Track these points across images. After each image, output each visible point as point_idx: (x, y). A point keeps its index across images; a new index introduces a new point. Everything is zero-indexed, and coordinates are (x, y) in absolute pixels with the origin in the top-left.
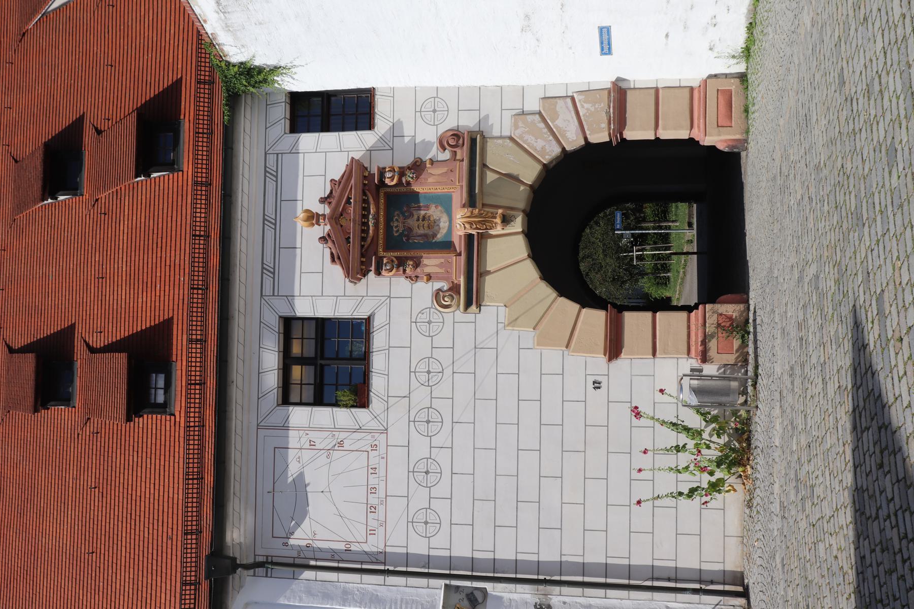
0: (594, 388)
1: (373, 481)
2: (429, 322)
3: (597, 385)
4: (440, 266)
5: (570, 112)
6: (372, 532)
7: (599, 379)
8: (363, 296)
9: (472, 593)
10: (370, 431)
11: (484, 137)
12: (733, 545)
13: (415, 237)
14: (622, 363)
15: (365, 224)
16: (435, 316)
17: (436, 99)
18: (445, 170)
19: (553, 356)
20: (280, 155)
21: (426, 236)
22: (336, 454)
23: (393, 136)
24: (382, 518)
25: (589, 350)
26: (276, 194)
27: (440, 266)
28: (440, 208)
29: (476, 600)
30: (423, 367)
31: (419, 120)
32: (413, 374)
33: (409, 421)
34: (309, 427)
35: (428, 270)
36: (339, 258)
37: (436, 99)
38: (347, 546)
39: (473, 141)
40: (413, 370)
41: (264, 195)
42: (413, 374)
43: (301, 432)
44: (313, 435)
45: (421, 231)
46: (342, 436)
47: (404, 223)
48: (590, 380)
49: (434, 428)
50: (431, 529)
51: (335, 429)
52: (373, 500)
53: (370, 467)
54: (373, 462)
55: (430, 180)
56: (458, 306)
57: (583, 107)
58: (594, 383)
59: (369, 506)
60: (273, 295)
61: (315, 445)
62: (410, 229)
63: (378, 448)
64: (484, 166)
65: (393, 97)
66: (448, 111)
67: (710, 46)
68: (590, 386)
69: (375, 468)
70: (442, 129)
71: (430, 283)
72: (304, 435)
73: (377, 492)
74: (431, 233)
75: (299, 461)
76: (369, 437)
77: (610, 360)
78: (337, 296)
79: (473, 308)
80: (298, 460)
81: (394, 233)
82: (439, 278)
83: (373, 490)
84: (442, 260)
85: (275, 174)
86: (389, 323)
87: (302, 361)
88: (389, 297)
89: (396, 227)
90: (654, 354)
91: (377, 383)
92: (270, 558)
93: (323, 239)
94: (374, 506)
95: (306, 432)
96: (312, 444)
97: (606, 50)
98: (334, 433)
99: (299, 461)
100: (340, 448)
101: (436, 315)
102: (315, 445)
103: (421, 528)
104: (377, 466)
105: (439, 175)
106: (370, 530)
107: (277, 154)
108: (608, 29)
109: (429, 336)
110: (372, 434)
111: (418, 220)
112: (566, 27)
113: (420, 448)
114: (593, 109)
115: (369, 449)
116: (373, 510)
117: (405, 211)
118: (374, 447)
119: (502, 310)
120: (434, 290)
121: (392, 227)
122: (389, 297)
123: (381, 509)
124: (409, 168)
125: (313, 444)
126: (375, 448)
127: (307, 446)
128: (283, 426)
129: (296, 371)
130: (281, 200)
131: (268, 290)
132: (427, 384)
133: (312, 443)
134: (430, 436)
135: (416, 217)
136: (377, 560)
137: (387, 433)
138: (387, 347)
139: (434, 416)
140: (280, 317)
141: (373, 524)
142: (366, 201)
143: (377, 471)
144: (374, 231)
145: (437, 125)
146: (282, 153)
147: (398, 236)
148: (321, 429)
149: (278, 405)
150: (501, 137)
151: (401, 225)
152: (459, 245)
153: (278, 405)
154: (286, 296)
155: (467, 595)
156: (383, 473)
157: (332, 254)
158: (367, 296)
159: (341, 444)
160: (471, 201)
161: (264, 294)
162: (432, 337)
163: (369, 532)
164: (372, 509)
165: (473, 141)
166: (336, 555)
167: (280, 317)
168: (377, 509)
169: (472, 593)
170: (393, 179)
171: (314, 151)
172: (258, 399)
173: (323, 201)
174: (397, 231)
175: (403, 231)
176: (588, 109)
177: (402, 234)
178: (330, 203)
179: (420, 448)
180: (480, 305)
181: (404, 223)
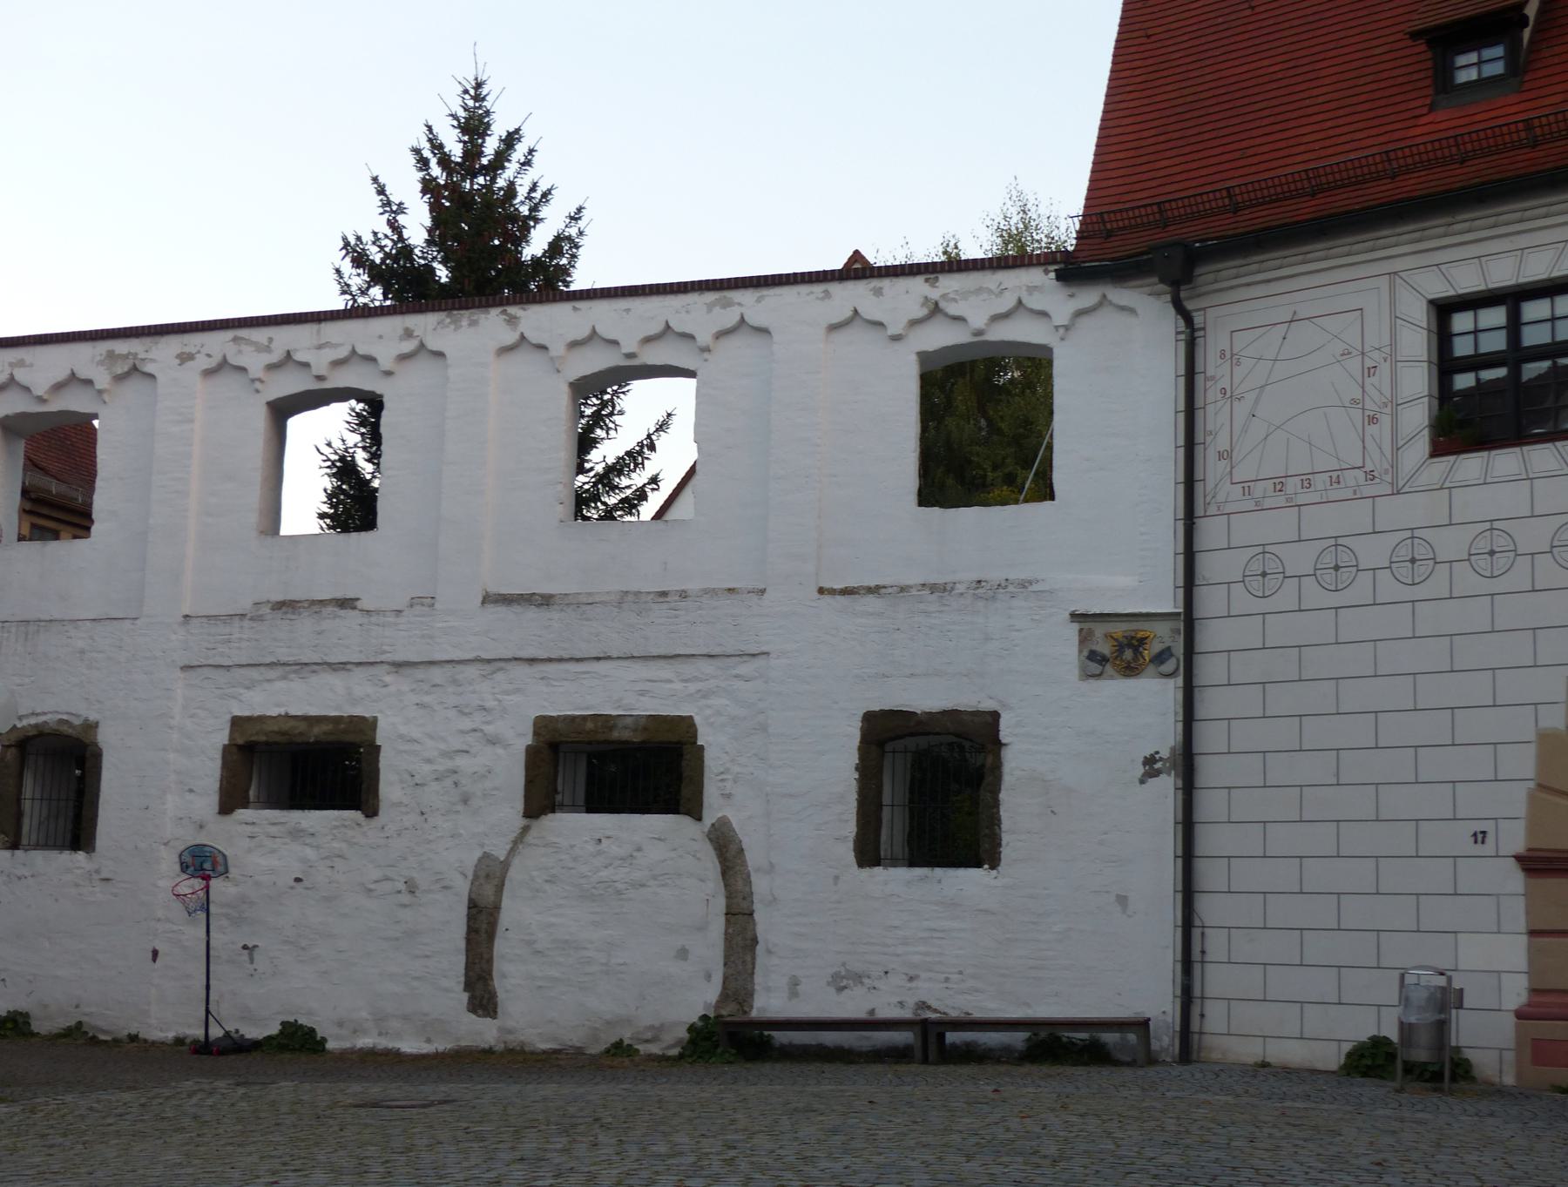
0: (1475, 835)
1: (1320, 481)
3: (1480, 837)
6: (1247, 489)
7: (1490, 839)
9: (1172, 655)
10: (1394, 466)
12: (1250, 1052)
14: (1516, 880)
19: (1523, 763)
22: (1357, 414)
24: (1268, 503)
25: (1533, 825)
29: (1162, 663)
30: (1501, 542)
34: (1396, 361)
38: (1225, 453)
40: (1496, 525)
43: (1387, 350)
44: (1385, 368)
46: (1386, 420)
48: (1488, 826)
49: (1404, 571)
51: (1395, 405)
52: (1292, 485)
53: (1339, 473)
54: (1350, 478)
58: (1484, 833)
59: (1283, 480)
63: (1370, 482)
68: (1480, 826)
69: (1339, 482)
72: (1384, 355)
73: (1305, 490)
75: (1342, 355)
76: (1387, 466)
83: (1307, 484)
87: (1514, 326)
91: (1471, 465)
92: (1201, 333)
94: (1283, 488)
95: (1389, 358)
99: (1342, 355)
102: (1369, 376)
104: (1342, 485)
106: (1249, 487)
110: (1391, 470)
113: (1372, 552)
115: (1368, 469)
116: (1278, 487)
118: (1371, 476)
123: (1281, 501)
125: (1371, 374)
126: (1368, 476)
127: (1369, 363)
129: (1495, 316)
133: (1372, 370)
136: (1209, 504)
137: (1393, 494)
138: (1531, 476)
139: (1422, 569)
141: (1258, 490)
143: (1335, 485)
155: (1169, 648)
156: (1333, 495)
159: (1373, 420)
163: (1246, 485)
164: (1280, 487)
166: (1212, 437)
168: (1280, 493)
169: (1172, 655)
172: (1437, 265)
179: (1372, 552)
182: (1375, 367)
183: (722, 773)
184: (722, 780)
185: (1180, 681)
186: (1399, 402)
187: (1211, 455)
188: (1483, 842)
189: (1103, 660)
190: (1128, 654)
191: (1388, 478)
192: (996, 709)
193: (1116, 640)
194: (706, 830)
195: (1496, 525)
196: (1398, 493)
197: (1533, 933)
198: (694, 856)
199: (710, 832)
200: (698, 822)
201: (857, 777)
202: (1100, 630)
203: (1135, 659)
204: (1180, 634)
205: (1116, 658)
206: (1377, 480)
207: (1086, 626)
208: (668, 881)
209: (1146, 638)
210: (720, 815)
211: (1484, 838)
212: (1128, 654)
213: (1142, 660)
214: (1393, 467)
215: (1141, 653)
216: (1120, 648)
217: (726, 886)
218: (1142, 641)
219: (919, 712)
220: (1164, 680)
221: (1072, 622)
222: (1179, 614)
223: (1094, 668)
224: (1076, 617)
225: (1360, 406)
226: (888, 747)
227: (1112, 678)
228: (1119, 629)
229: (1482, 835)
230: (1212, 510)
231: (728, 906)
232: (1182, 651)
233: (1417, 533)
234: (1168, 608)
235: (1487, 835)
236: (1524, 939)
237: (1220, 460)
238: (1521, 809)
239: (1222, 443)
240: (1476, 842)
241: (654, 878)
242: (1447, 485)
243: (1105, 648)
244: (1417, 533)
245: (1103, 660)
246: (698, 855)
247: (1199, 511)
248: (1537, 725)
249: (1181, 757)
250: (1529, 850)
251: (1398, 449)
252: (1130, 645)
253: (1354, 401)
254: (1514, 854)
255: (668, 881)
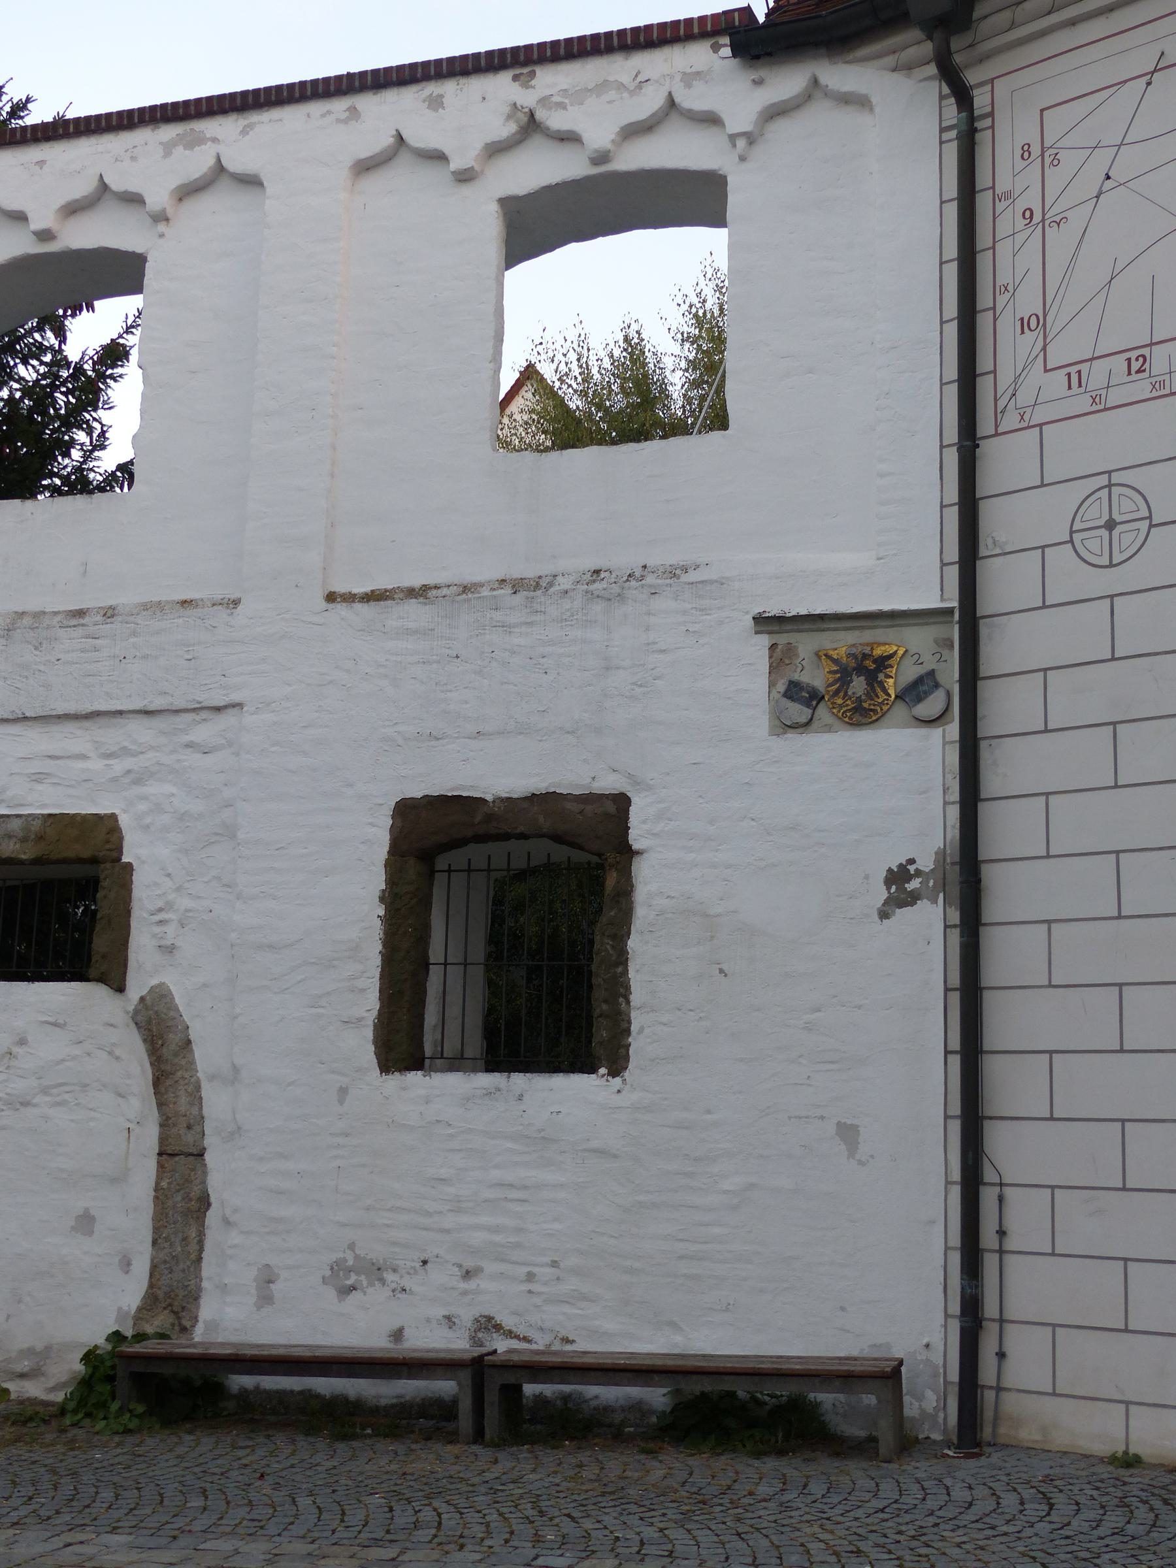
9: (937, 685)
29: (919, 699)
50: (1094, 544)
94: (1147, 365)
103: (1096, 513)
116: (1135, 366)
123: (1142, 388)
141: (1097, 375)
155: (932, 673)
168: (1141, 375)
169: (937, 685)
183: (160, 910)
184: (161, 922)
185: (953, 729)
187: (1007, 325)
189: (813, 698)
190: (858, 685)
192: (623, 790)
193: (835, 661)
194: (131, 1008)
198: (110, 1053)
199: (136, 1012)
200: (118, 994)
201: (382, 913)
202: (807, 644)
203: (871, 694)
204: (952, 646)
205: (837, 693)
207: (782, 639)
208: (66, 1096)
209: (891, 656)
210: (154, 982)
212: (858, 685)
213: (882, 696)
215: (881, 684)
216: (844, 675)
217: (160, 1105)
218: (883, 662)
219: (489, 798)
220: (923, 731)
221: (756, 633)
222: (949, 612)
223: (799, 713)
224: (764, 623)
226: (441, 863)
227: (829, 729)
228: (842, 643)
230: (1010, 421)
231: (163, 1140)
232: (957, 676)
234: (932, 601)
237: (1023, 332)
239: (1028, 303)
241: (45, 1091)
243: (816, 678)
245: (813, 698)
246: (117, 1052)
247: (985, 426)
249: (957, 868)
252: (860, 669)
255: (66, 1096)
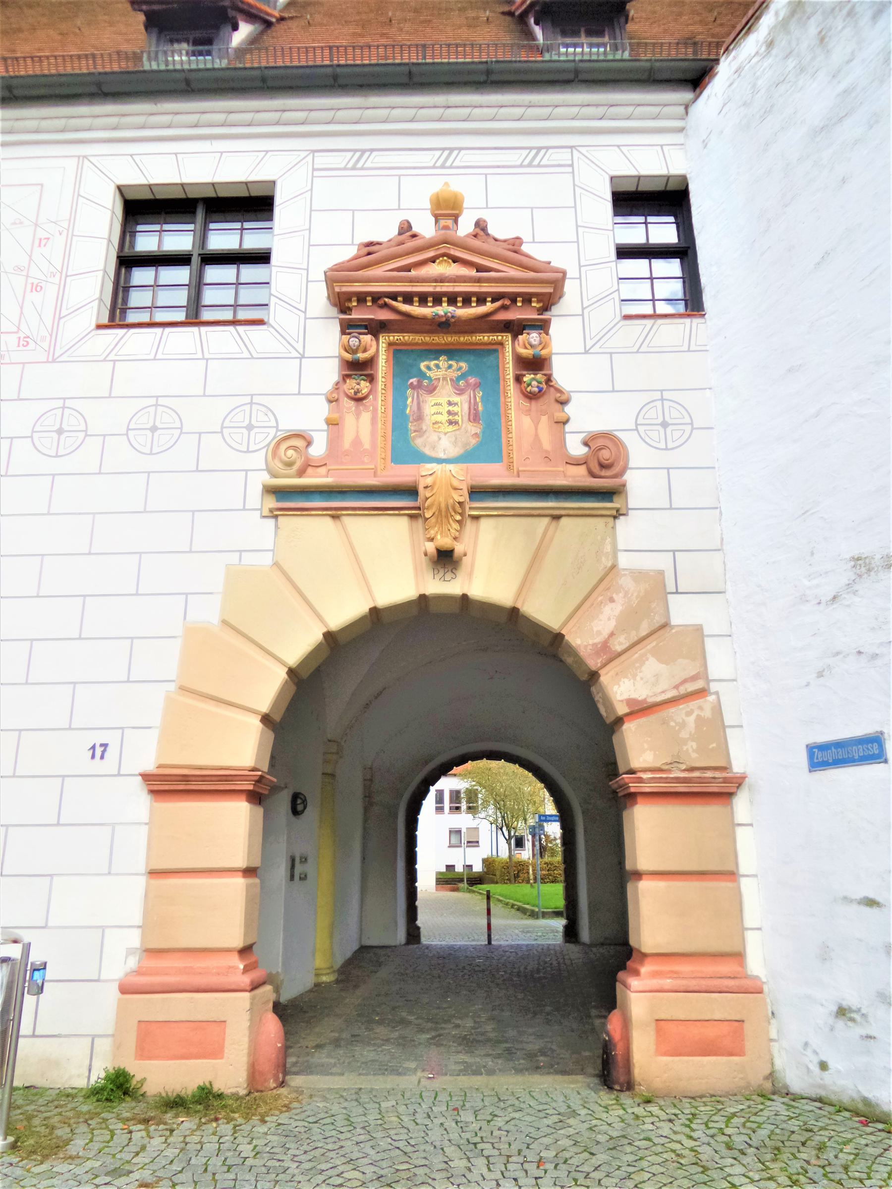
2: (250, 427)
3: (99, 751)
4: (357, 442)
5: (676, 687)
8: (305, 312)
11: (615, 517)
13: (418, 396)
15: (437, 299)
16: (260, 437)
17: (689, 427)
18: (547, 445)
20: (570, 169)
21: (420, 418)
23: (611, 354)
26: (498, 167)
27: (357, 442)
28: (473, 441)
31: (645, 398)
32: (153, 401)
33: (64, 399)
34: (73, 235)
35: (349, 421)
36: (369, 254)
37: (689, 427)
39: (608, 494)
40: (161, 401)
41: (495, 148)
42: (153, 401)
43: (66, 225)
45: (429, 409)
46: (51, 291)
47: (445, 379)
55: (527, 421)
56: (274, 476)
57: (689, 714)
58: (105, 746)
60: (314, 170)
61: (40, 245)
62: (431, 390)
63: (21, 348)
64: (557, 518)
65: (689, 351)
66: (666, 449)
67: (851, 1010)
70: (626, 438)
71: (325, 427)
72: (61, 229)
74: (424, 428)
75: (15, 223)
77: (147, 777)
78: (307, 270)
79: (272, 503)
80: (18, 222)
81: (425, 363)
82: (334, 442)
84: (367, 445)
85: (536, 162)
86: (253, 358)
88: (303, 356)
89: (437, 366)
90: (154, 873)
93: (406, 228)
95: (65, 232)
96: (42, 242)
97: (819, 756)
98: (58, 275)
99: (15, 223)
100: (29, 286)
101: (264, 438)
102: (40, 245)
105: (537, 435)
107: (572, 165)
108: (879, 757)
109: (222, 427)
110: (48, 336)
111: (450, 403)
112: (875, 656)
114: (684, 734)
117: (467, 382)
119: (267, 559)
120: (311, 433)
121: (437, 359)
122: (303, 356)
124: (549, 379)
126: (22, 342)
127: (41, 234)
128: (79, 195)
130: (486, 175)
131: (322, 160)
132: (132, 426)
133: (43, 242)
134: (32, 437)
135: (456, 399)
137: (47, 362)
138: (207, 356)
140: (274, 182)
142: (481, 299)
144: (423, 319)
145: (637, 430)
146: (573, 172)
147: (420, 370)
148: (67, 253)
149: (120, 188)
150: (615, 551)
151: (440, 374)
152: (400, 474)
153: (120, 188)
154: (311, 190)
157: (379, 244)
158: (306, 318)
159: (36, 288)
160: (478, 492)
161: (316, 154)
162: (222, 432)
165: (608, 494)
167: (274, 182)
170: (526, 348)
171: (579, 224)
173: (480, 225)
174: (429, 368)
175: (429, 378)
176: (683, 725)
177: (422, 375)
178: (475, 236)
180: (276, 517)
181: (445, 379)
182: (48, 239)
186: (68, 274)
188: (102, 757)
191: (46, 345)
195: (161, 401)
196: (54, 361)
197: (154, 873)
206: (32, 345)
211: (103, 752)
214: (51, 336)
225: (24, 273)
229: (102, 749)
233: (68, 403)
235: (108, 749)
236: (142, 880)
238: (156, 719)
240: (93, 757)
242: (111, 357)
244: (68, 403)
248: (185, 618)
250: (159, 767)
251: (60, 318)
253: (19, 268)
254: (141, 771)
